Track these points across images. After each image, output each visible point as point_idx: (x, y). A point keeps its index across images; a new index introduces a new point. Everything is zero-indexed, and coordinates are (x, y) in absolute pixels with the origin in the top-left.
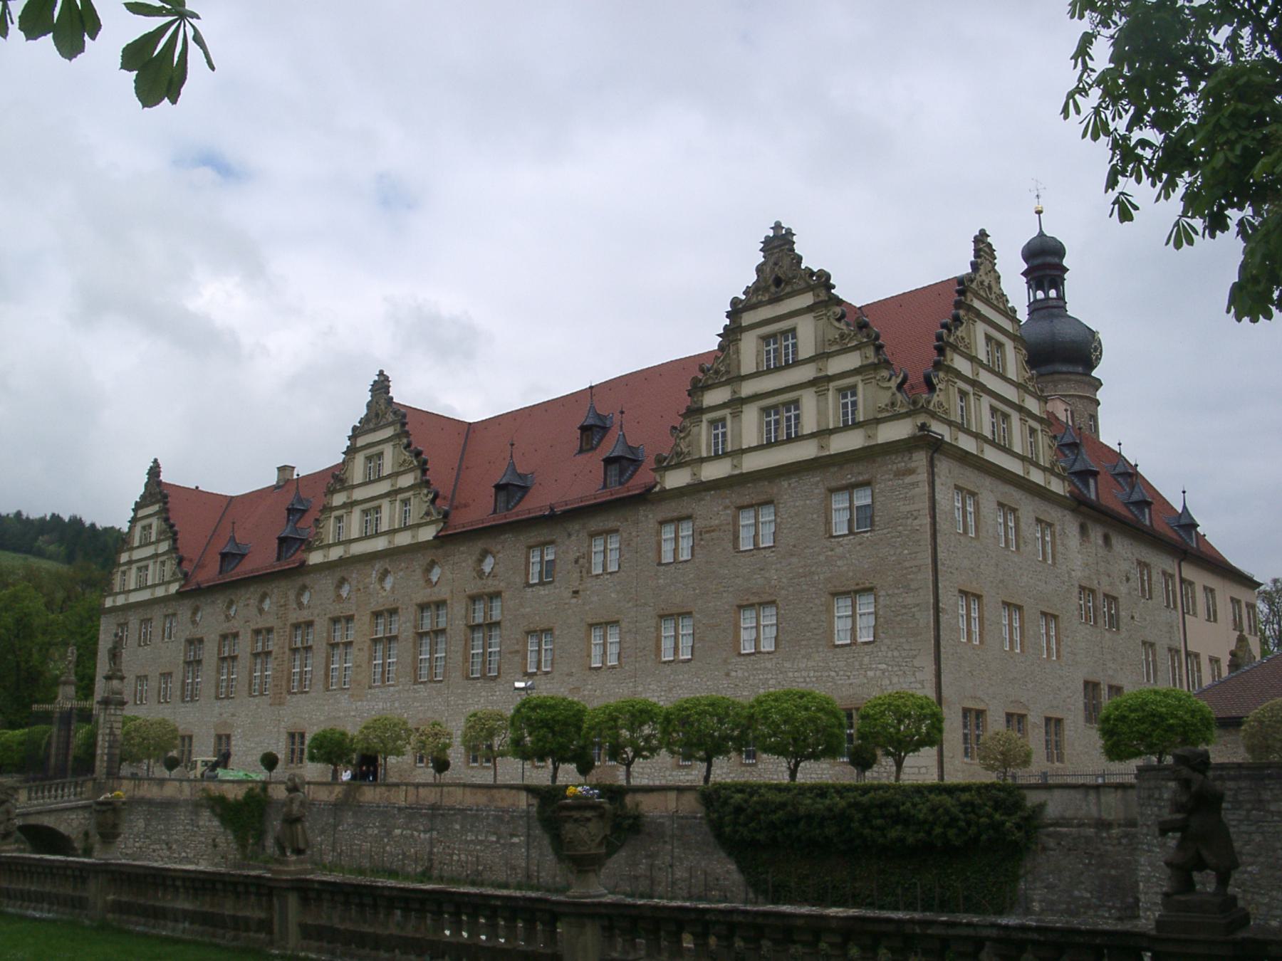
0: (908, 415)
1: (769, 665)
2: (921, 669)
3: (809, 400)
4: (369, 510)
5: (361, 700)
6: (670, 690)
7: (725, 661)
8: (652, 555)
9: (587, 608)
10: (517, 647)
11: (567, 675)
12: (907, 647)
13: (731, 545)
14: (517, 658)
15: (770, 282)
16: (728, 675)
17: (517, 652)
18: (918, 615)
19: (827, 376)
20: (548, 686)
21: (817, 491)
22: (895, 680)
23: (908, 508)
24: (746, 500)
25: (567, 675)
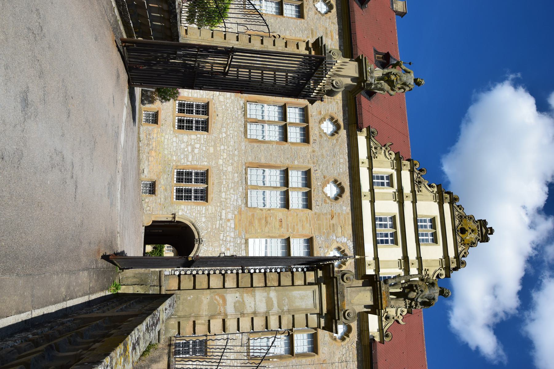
4: (395, 228)
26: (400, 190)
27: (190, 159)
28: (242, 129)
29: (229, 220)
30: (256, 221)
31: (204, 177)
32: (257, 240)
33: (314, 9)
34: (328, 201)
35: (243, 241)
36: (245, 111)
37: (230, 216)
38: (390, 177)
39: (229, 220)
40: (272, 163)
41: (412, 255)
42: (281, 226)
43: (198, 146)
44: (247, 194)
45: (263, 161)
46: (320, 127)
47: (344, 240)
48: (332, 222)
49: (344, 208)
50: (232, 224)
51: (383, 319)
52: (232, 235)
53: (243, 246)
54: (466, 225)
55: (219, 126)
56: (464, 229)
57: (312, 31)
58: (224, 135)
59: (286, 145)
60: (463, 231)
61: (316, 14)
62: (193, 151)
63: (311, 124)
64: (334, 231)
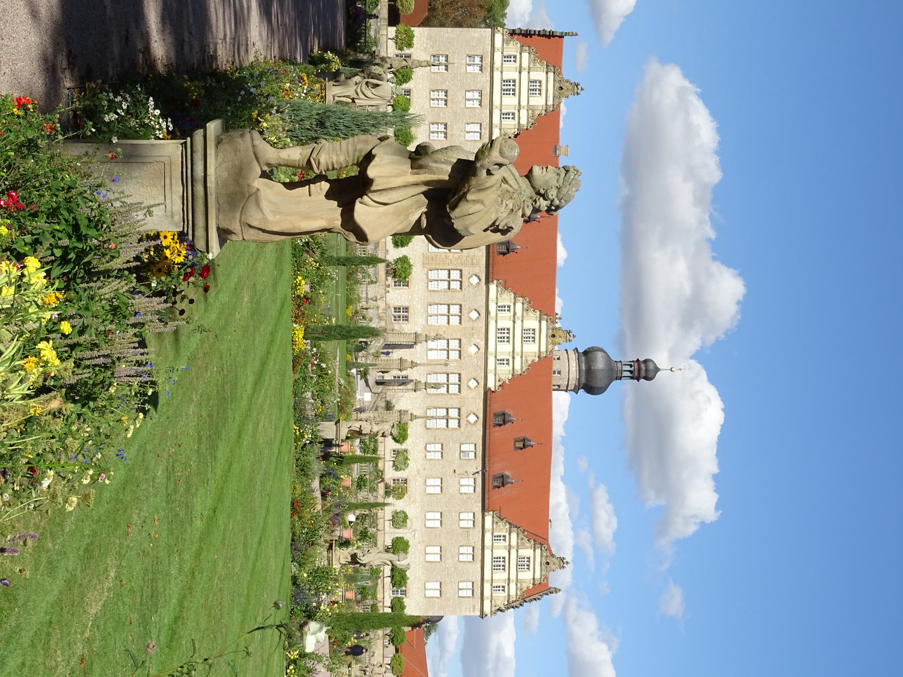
0: (491, 611)
1: (421, 559)
3: (505, 576)
6: (416, 518)
7: (424, 542)
8: (463, 510)
9: (448, 478)
10: (437, 439)
14: (432, 439)
15: (548, 561)
16: (419, 543)
17: (435, 440)
22: (414, 604)
28: (426, 285)
31: (406, 309)
36: (428, 275)
40: (442, 303)
41: (518, 349)
45: (436, 302)
46: (469, 282)
47: (478, 341)
51: (497, 380)
54: (557, 333)
59: (450, 293)
60: (554, 336)
62: (401, 297)
63: (463, 281)
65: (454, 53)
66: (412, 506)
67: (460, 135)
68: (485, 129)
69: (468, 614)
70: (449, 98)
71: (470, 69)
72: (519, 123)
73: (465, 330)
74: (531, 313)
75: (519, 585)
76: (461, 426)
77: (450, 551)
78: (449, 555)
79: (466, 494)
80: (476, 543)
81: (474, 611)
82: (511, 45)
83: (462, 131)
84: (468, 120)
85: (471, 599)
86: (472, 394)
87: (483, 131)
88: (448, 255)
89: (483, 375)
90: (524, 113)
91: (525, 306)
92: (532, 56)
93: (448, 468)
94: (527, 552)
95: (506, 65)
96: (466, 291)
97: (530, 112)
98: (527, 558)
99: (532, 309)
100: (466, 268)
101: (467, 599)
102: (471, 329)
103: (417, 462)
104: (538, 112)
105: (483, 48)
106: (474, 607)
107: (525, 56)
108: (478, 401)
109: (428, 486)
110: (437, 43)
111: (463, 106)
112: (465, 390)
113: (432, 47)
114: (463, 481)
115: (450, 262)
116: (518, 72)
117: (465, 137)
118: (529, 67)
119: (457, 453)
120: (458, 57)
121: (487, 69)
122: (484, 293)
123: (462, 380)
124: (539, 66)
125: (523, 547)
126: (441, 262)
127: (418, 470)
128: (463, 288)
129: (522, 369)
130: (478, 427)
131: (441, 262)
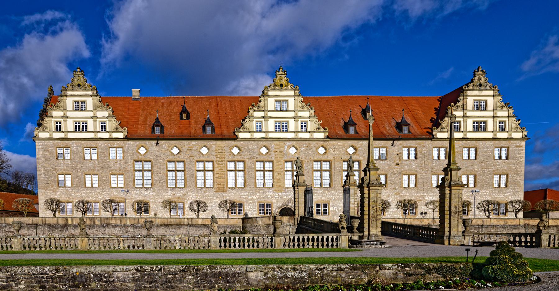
2: (520, 195)
4: (280, 122)
5: (282, 192)
9: (403, 169)
11: (394, 189)
12: (517, 189)
13: (461, 157)
15: (478, 84)
18: (520, 182)
19: (498, 116)
20: (385, 192)
21: (491, 147)
23: (519, 156)
24: (468, 146)
25: (394, 189)
26: (263, 117)
27: (255, 210)
28: (241, 189)
29: (279, 195)
30: (279, 184)
32: (286, 183)
33: (178, 155)
34: (269, 153)
35: (287, 189)
37: (277, 194)
38: (257, 122)
39: (279, 195)
40: (254, 177)
41: (292, 114)
42: (280, 174)
43: (249, 207)
44: (268, 188)
45: (254, 181)
47: (286, 147)
48: (278, 152)
49: (272, 146)
50: (280, 194)
52: (284, 193)
53: (289, 189)
55: (240, 199)
56: (280, 84)
57: (190, 157)
58: (244, 196)
59: (246, 170)
61: (181, 154)
62: (252, 209)
63: (237, 160)
64: (282, 151)
65: (56, 169)
66: (426, 198)
67: (120, 164)
68: (114, 144)
69: (524, 151)
70: (91, 172)
71: (67, 157)
72: (107, 117)
73: (277, 158)
74: (261, 104)
75: (498, 109)
76: (358, 159)
77: (467, 167)
78: (470, 168)
79: (416, 155)
80: (461, 145)
81: (521, 147)
82: (47, 126)
83: (116, 163)
84: (108, 158)
85: (510, 149)
86: (331, 151)
87: (115, 146)
88: (215, 172)
89: (314, 143)
90: (99, 114)
91: (256, 109)
92: (55, 109)
93: (395, 170)
94: (470, 102)
95: (63, 129)
96: (245, 157)
97: (99, 109)
98: (475, 103)
99: (259, 103)
100: (226, 157)
101: (510, 152)
102: (276, 153)
103: (389, 195)
104: (98, 104)
105: (51, 147)
106: (517, 146)
107: (55, 114)
108: (337, 147)
109: (409, 186)
110: (49, 182)
111: (96, 162)
112: (327, 157)
113: (52, 186)
114: (405, 157)
115: (221, 171)
116: (68, 119)
117: (121, 160)
118: (62, 111)
119: (381, 162)
120: (59, 167)
121: (67, 144)
122: (246, 143)
123: (319, 159)
124: (62, 104)
125: (465, 106)
126: (222, 177)
127: (396, 194)
128: (243, 159)
129: (309, 111)
130: (359, 146)
131: (222, 177)
